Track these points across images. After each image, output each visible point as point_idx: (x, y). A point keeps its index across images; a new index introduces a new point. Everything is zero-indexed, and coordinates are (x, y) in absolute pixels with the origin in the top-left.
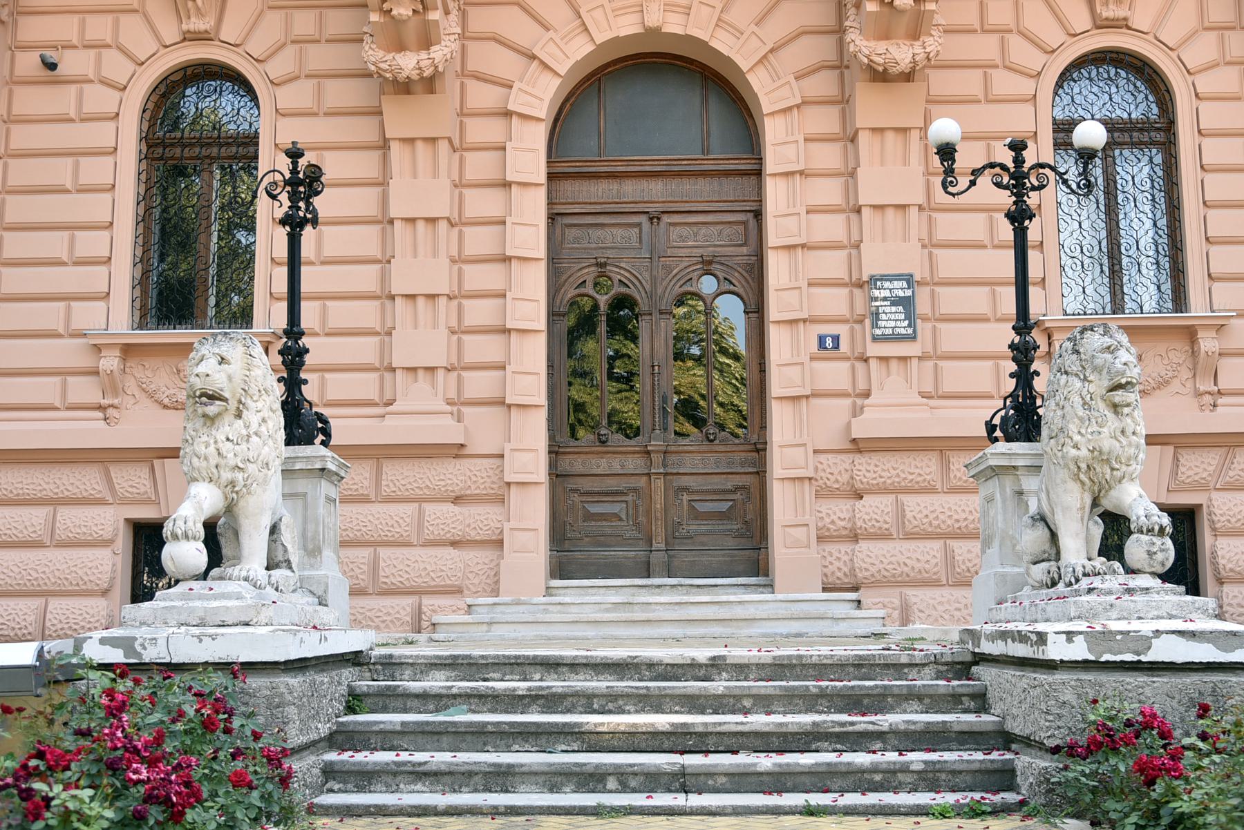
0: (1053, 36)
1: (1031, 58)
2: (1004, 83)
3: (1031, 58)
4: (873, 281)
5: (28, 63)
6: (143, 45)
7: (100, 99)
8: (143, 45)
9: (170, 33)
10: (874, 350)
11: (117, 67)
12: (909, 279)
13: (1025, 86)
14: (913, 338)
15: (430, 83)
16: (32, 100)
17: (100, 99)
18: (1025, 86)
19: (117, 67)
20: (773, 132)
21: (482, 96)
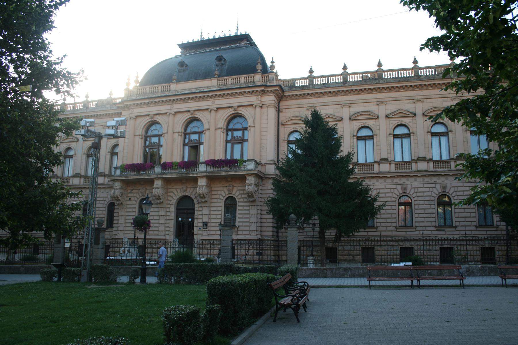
0: (224, 195)
1: (221, 198)
2: (219, 201)
3: (221, 198)
4: (204, 222)
5: (128, 198)
6: (138, 197)
7: (135, 202)
8: (138, 197)
9: (141, 195)
10: (203, 230)
11: (136, 199)
12: (207, 222)
13: (221, 201)
14: (207, 228)
15: (162, 202)
16: (129, 202)
17: (135, 202)
18: (221, 201)
19: (136, 199)
20: (196, 206)
21: (169, 202)
